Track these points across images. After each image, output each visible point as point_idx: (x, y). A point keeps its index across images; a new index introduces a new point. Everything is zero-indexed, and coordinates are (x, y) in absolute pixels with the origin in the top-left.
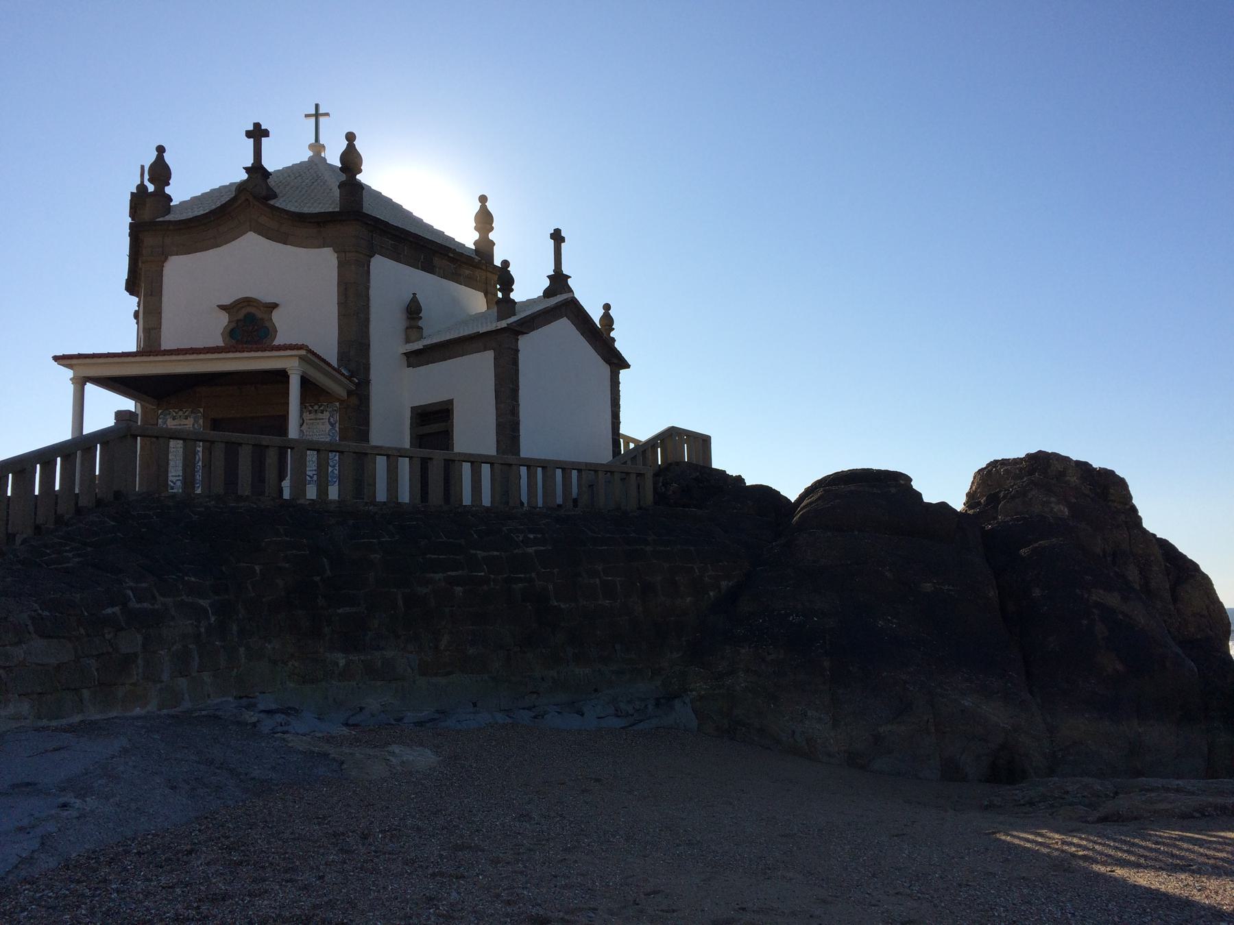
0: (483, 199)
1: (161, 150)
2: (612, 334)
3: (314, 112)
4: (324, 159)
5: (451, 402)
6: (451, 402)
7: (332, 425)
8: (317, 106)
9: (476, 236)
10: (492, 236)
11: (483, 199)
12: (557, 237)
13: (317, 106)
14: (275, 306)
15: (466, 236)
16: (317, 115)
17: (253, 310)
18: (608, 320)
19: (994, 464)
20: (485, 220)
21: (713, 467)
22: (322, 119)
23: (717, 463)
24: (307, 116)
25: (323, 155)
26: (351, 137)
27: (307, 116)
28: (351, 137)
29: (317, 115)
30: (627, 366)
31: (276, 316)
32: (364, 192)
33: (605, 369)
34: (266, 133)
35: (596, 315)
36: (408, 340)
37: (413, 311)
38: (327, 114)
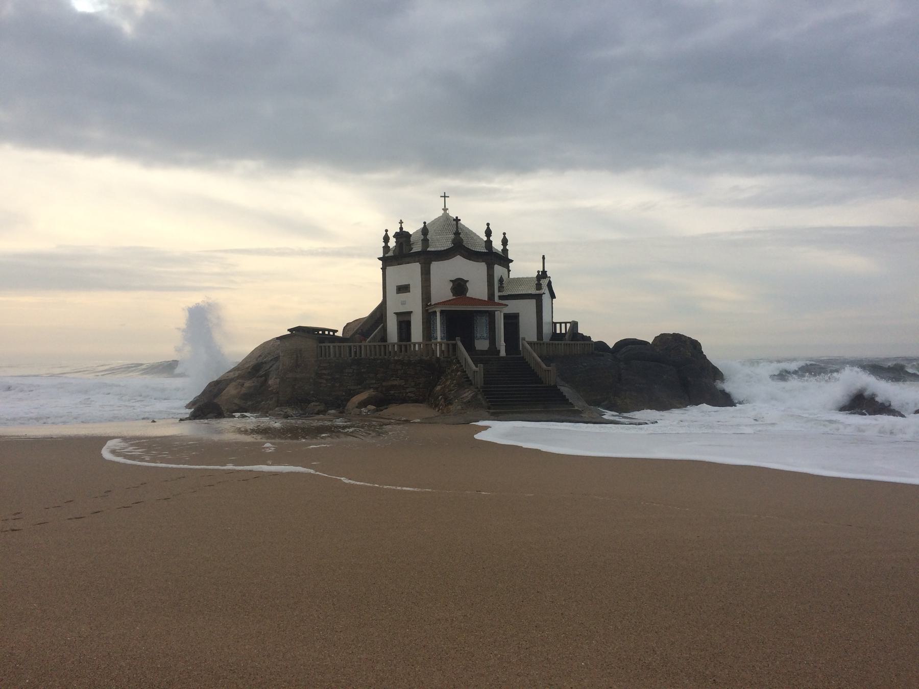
0: (504, 234)
1: (425, 223)
4: (448, 214)
5: (518, 313)
6: (518, 313)
7: (487, 321)
8: (445, 193)
10: (507, 247)
11: (504, 234)
12: (544, 256)
13: (445, 193)
14: (468, 281)
17: (459, 281)
19: (662, 334)
20: (505, 242)
21: (579, 332)
23: (581, 330)
24: (441, 197)
26: (488, 224)
27: (441, 197)
28: (488, 224)
29: (445, 197)
30: (555, 298)
33: (551, 300)
34: (460, 220)
36: (499, 291)
38: (448, 197)
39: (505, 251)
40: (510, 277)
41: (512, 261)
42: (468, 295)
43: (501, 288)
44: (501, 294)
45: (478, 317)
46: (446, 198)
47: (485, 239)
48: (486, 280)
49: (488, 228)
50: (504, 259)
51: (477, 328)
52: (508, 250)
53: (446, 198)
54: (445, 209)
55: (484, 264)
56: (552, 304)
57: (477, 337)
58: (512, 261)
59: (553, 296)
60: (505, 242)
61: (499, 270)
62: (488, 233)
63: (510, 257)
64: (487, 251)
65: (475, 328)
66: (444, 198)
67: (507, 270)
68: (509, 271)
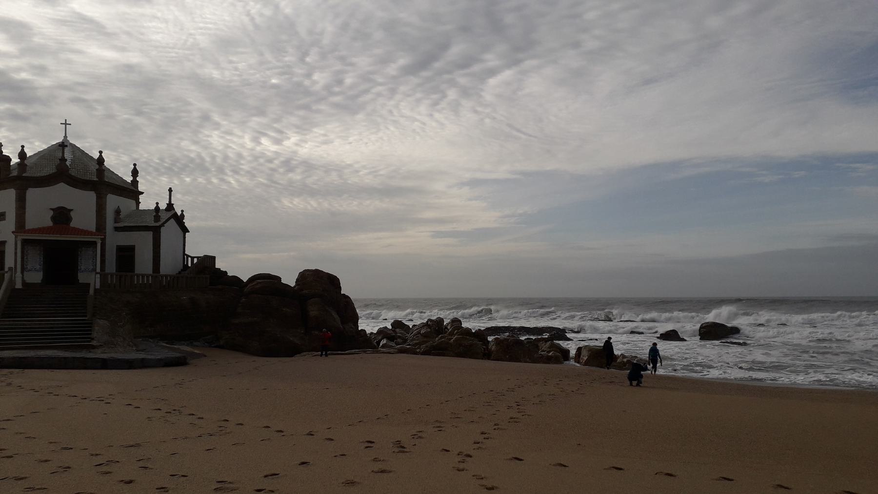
2: (184, 221)
3: (67, 123)
8: (66, 120)
9: (131, 178)
10: (138, 179)
13: (66, 120)
14: (72, 210)
15: (129, 179)
16: (66, 124)
18: (182, 216)
20: (135, 173)
22: (67, 126)
25: (68, 139)
30: (189, 232)
31: (72, 214)
32: (106, 173)
35: (179, 213)
36: (116, 222)
37: (118, 212)
39: (135, 183)
40: (140, 209)
41: (142, 193)
42: (72, 224)
43: (116, 220)
44: (118, 225)
45: (83, 248)
46: (67, 126)
47: (97, 167)
48: (94, 208)
49: (101, 156)
50: (132, 191)
51: (81, 259)
52: (138, 181)
53: (64, 122)
54: (66, 137)
55: (94, 192)
56: (184, 238)
57: (80, 269)
58: (142, 193)
59: (185, 230)
60: (135, 173)
61: (113, 201)
62: (101, 160)
63: (141, 188)
64: (97, 180)
65: (79, 260)
66: (64, 122)
67: (135, 201)
68: (138, 203)
